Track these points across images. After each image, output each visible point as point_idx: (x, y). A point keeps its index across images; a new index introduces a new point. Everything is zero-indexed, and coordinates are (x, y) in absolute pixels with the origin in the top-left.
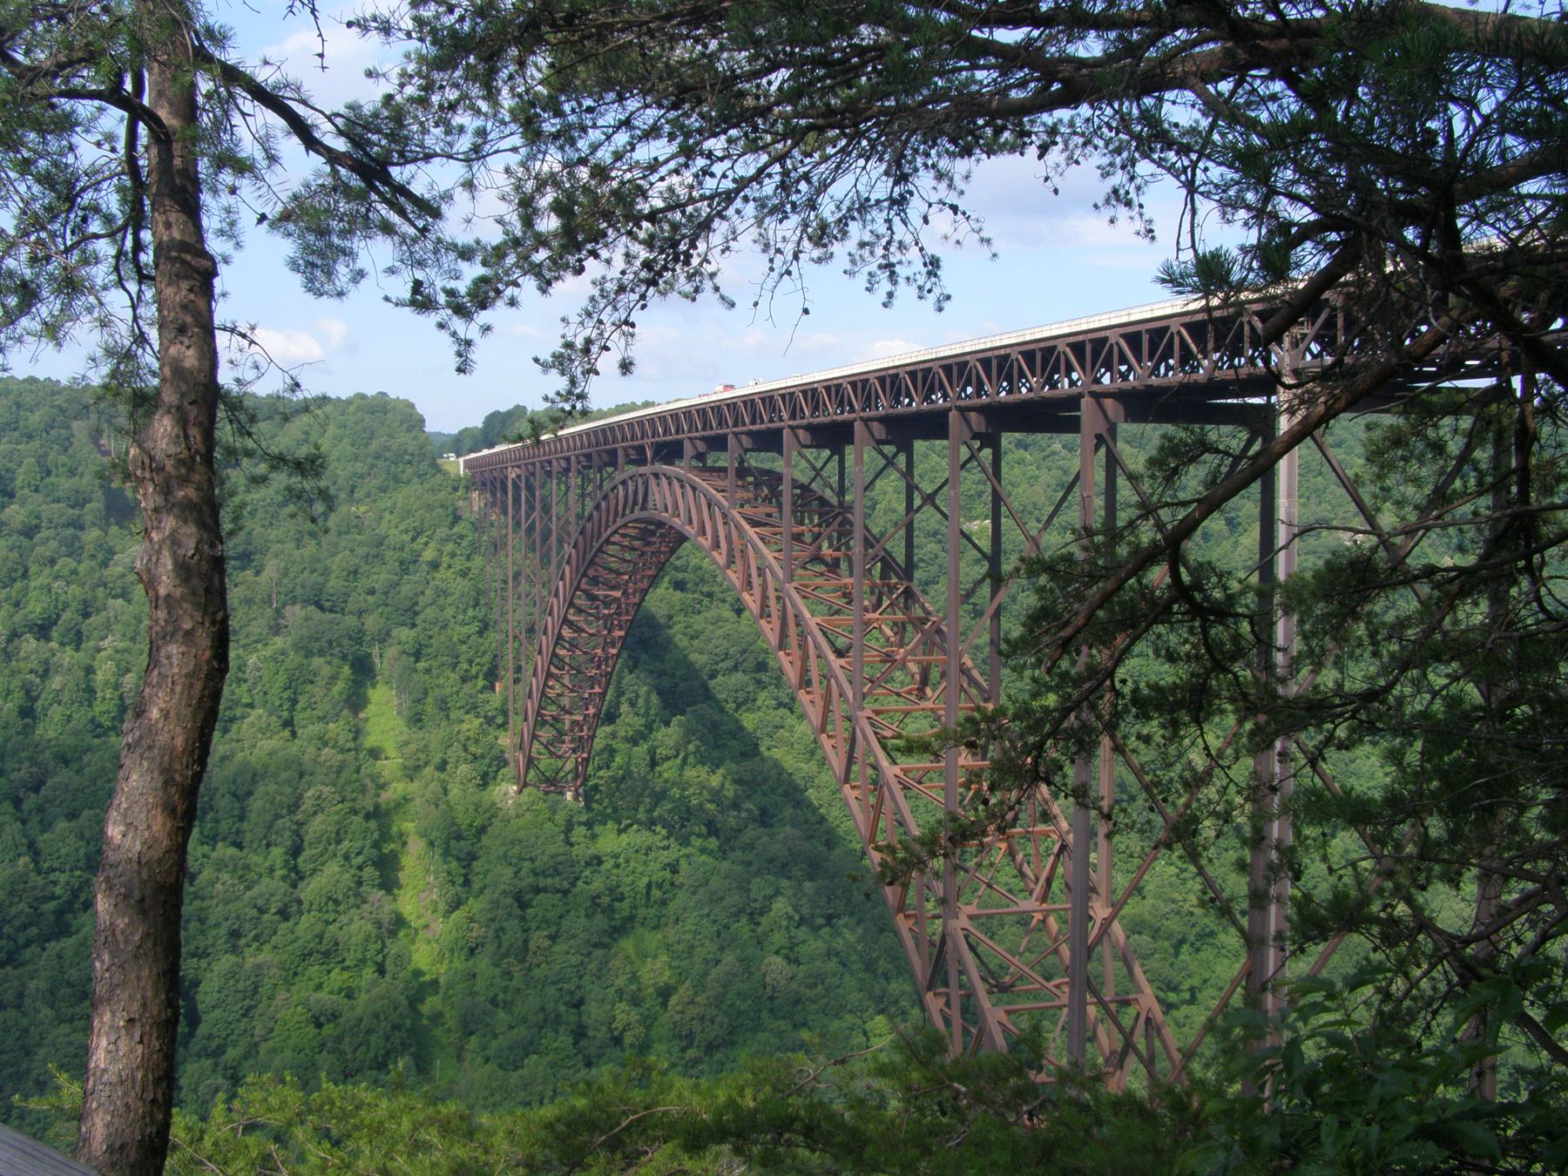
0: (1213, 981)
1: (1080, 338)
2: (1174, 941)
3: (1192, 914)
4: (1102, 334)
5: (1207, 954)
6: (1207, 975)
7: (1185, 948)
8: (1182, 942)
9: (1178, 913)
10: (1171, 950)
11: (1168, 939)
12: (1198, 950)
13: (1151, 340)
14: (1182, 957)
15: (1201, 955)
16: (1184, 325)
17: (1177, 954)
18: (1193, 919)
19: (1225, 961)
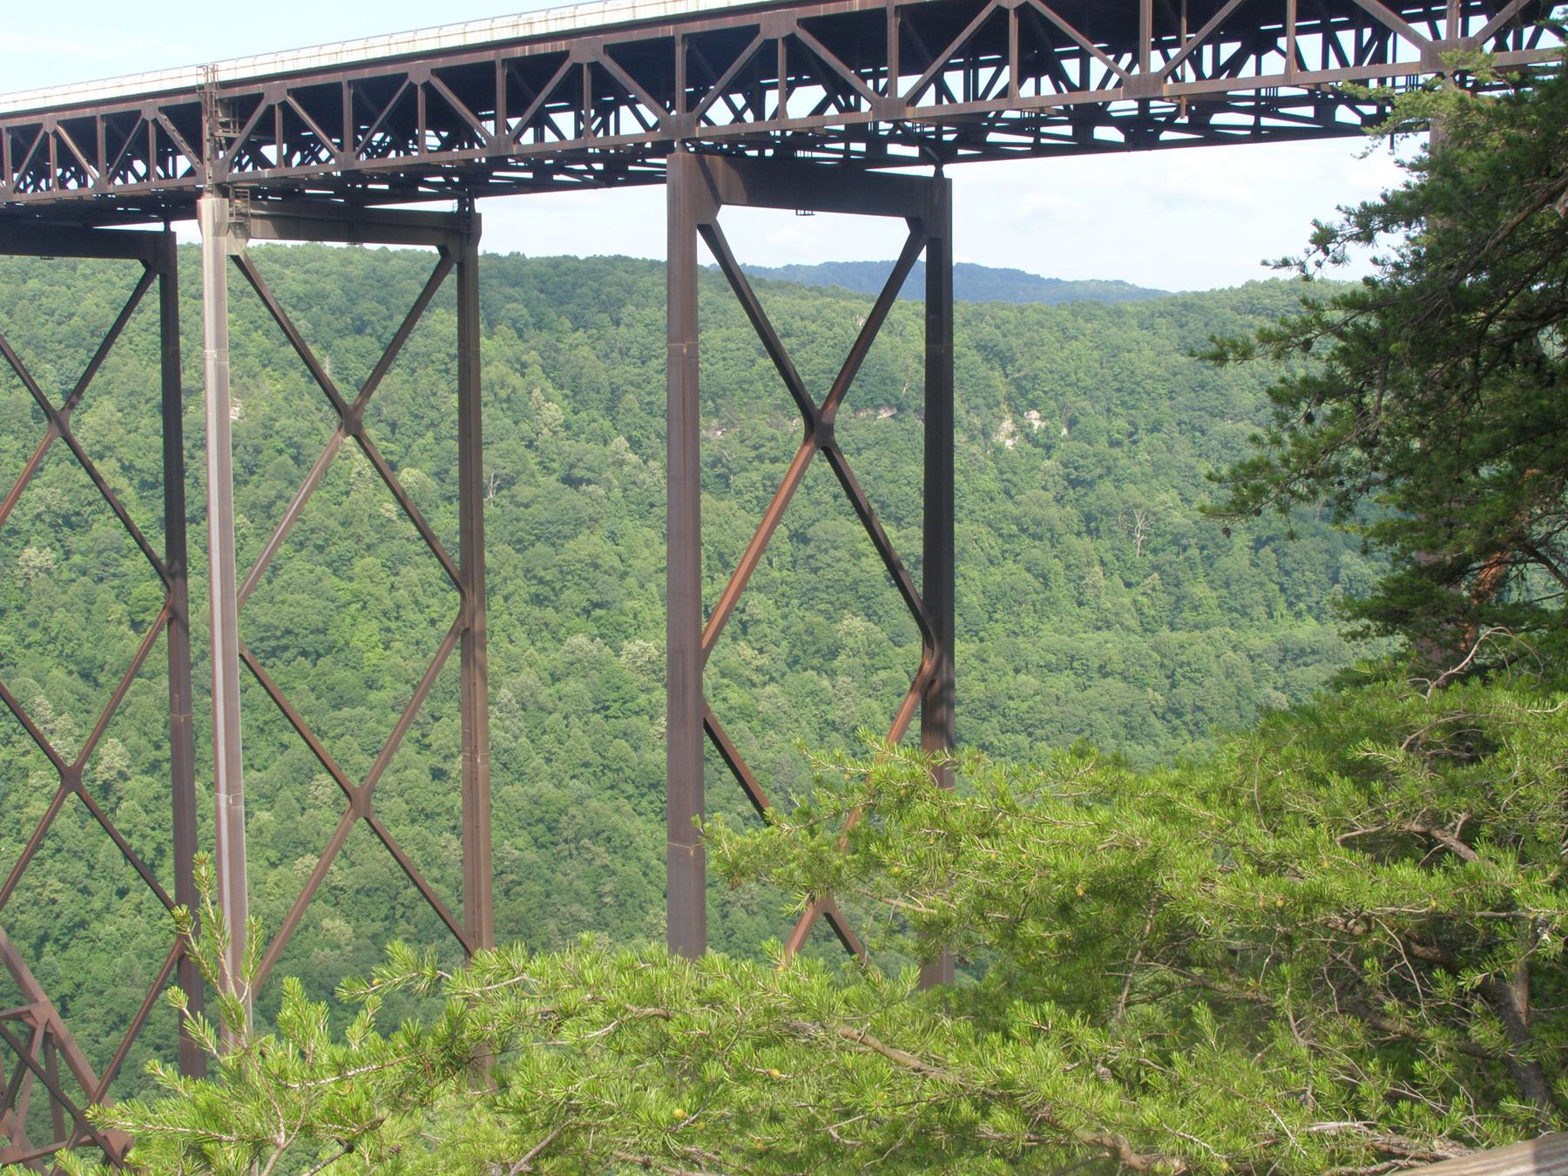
0: (88, 984)
1: (88, 112)
2: (34, 940)
3: (54, 902)
4: (34, 120)
5: (78, 950)
6: (80, 978)
7: (48, 947)
8: (44, 939)
9: (36, 903)
10: (31, 952)
11: (24, 938)
12: (65, 947)
13: (109, 130)
14: (45, 959)
15: (71, 952)
16: (63, 123)
17: (38, 957)
18: (56, 908)
19: (104, 956)
